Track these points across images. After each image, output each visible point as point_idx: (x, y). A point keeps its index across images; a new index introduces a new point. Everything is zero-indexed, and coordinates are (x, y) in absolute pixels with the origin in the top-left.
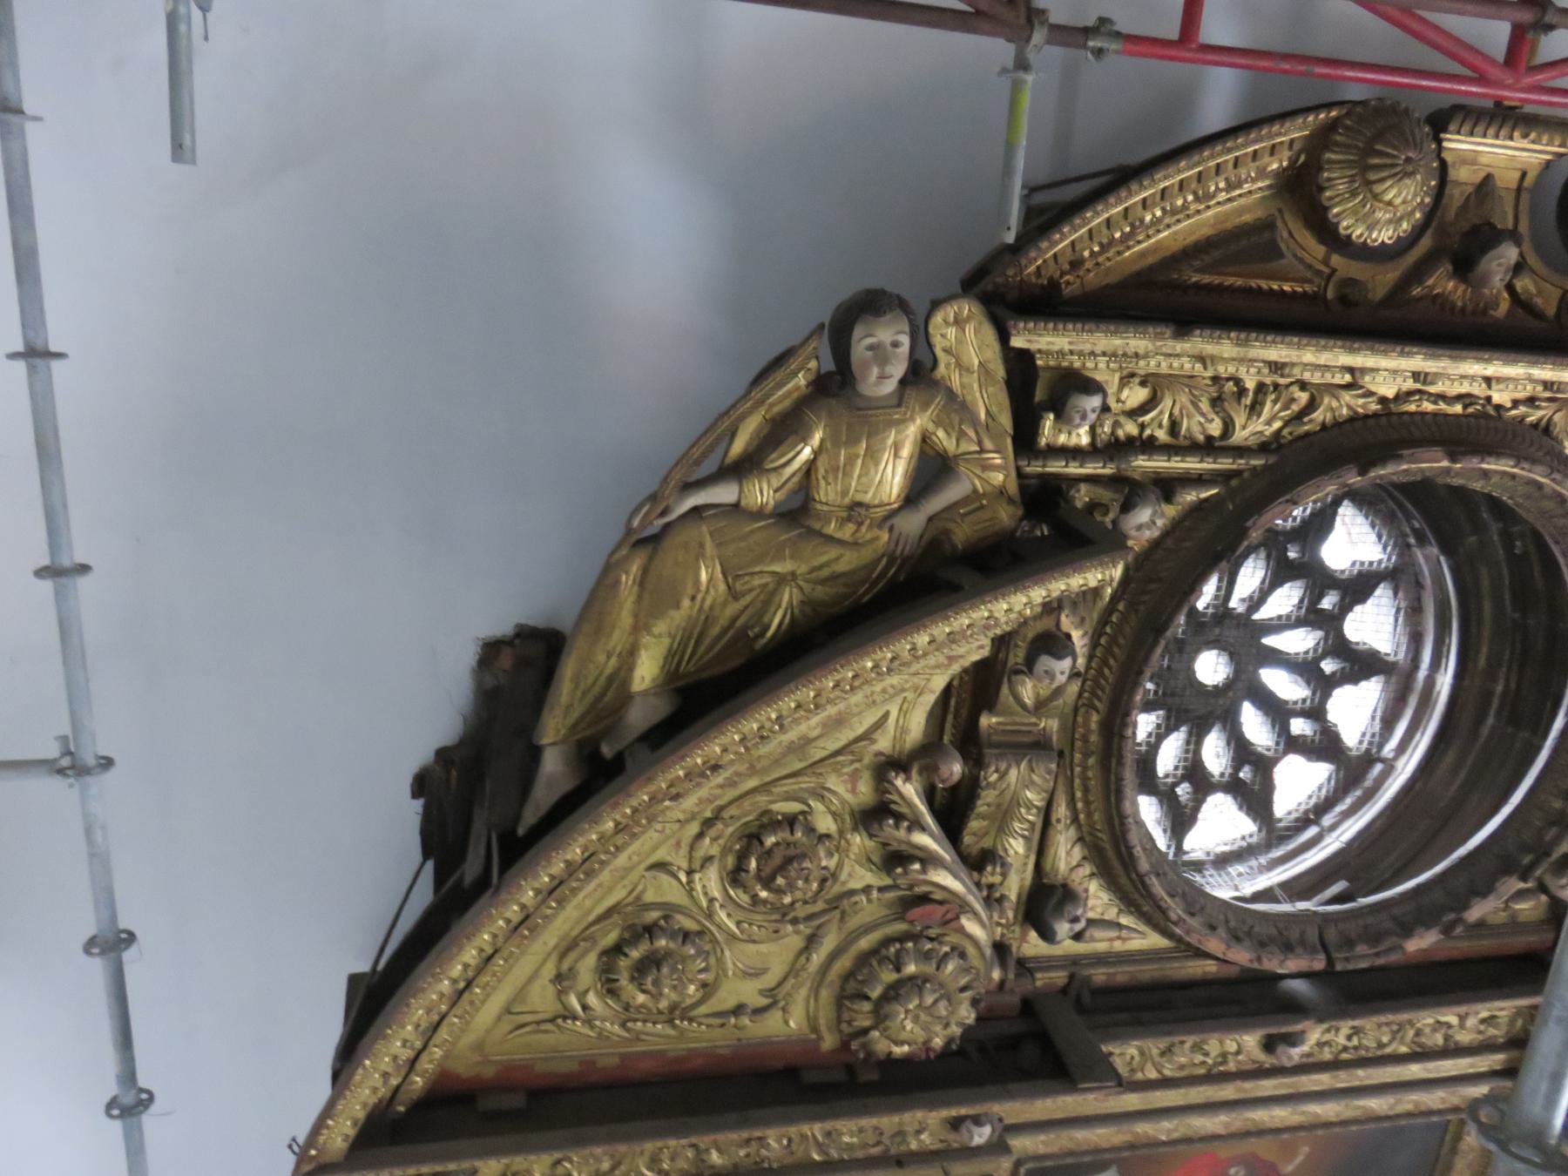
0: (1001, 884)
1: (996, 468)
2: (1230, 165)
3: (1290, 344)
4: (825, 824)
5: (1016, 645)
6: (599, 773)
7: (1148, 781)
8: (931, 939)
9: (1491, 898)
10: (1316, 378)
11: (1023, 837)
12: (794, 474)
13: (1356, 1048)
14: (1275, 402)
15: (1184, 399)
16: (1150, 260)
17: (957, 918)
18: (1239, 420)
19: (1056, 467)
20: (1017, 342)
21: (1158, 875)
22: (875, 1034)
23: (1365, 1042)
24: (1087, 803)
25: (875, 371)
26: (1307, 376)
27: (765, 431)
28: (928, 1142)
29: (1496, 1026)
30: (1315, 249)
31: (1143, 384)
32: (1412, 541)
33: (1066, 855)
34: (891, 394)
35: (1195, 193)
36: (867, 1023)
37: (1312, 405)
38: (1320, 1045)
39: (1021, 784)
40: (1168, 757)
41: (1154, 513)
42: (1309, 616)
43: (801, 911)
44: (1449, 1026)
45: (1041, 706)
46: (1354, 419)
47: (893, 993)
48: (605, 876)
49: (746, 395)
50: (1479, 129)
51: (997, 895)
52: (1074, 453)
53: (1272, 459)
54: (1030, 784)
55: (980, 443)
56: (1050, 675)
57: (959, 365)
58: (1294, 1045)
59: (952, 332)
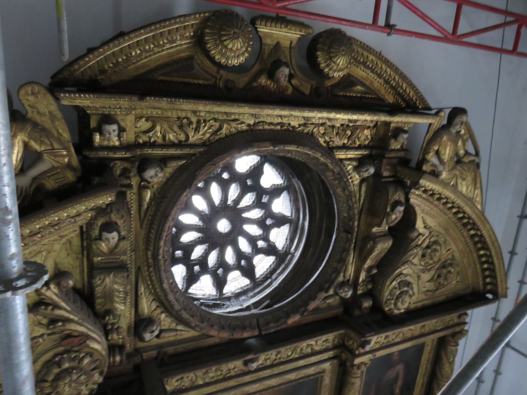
0: (118, 322)
1: (64, 156)
2: (167, 33)
3: (190, 103)
5: (94, 229)
9: (316, 300)
10: (220, 117)
11: (122, 303)
13: (280, 358)
14: (204, 127)
15: (166, 126)
16: (141, 71)
17: (85, 342)
18: (191, 134)
19: (104, 154)
20: (65, 102)
21: (185, 310)
23: (282, 356)
24: (153, 286)
26: (216, 116)
29: (329, 342)
32: (291, 176)
35: (153, 44)
37: (220, 128)
38: (266, 360)
44: (312, 345)
47: (58, 378)
50: (273, 25)
51: (116, 327)
52: (114, 149)
53: (206, 149)
54: (116, 283)
55: (52, 145)
57: (39, 113)
58: (253, 362)
59: (31, 98)
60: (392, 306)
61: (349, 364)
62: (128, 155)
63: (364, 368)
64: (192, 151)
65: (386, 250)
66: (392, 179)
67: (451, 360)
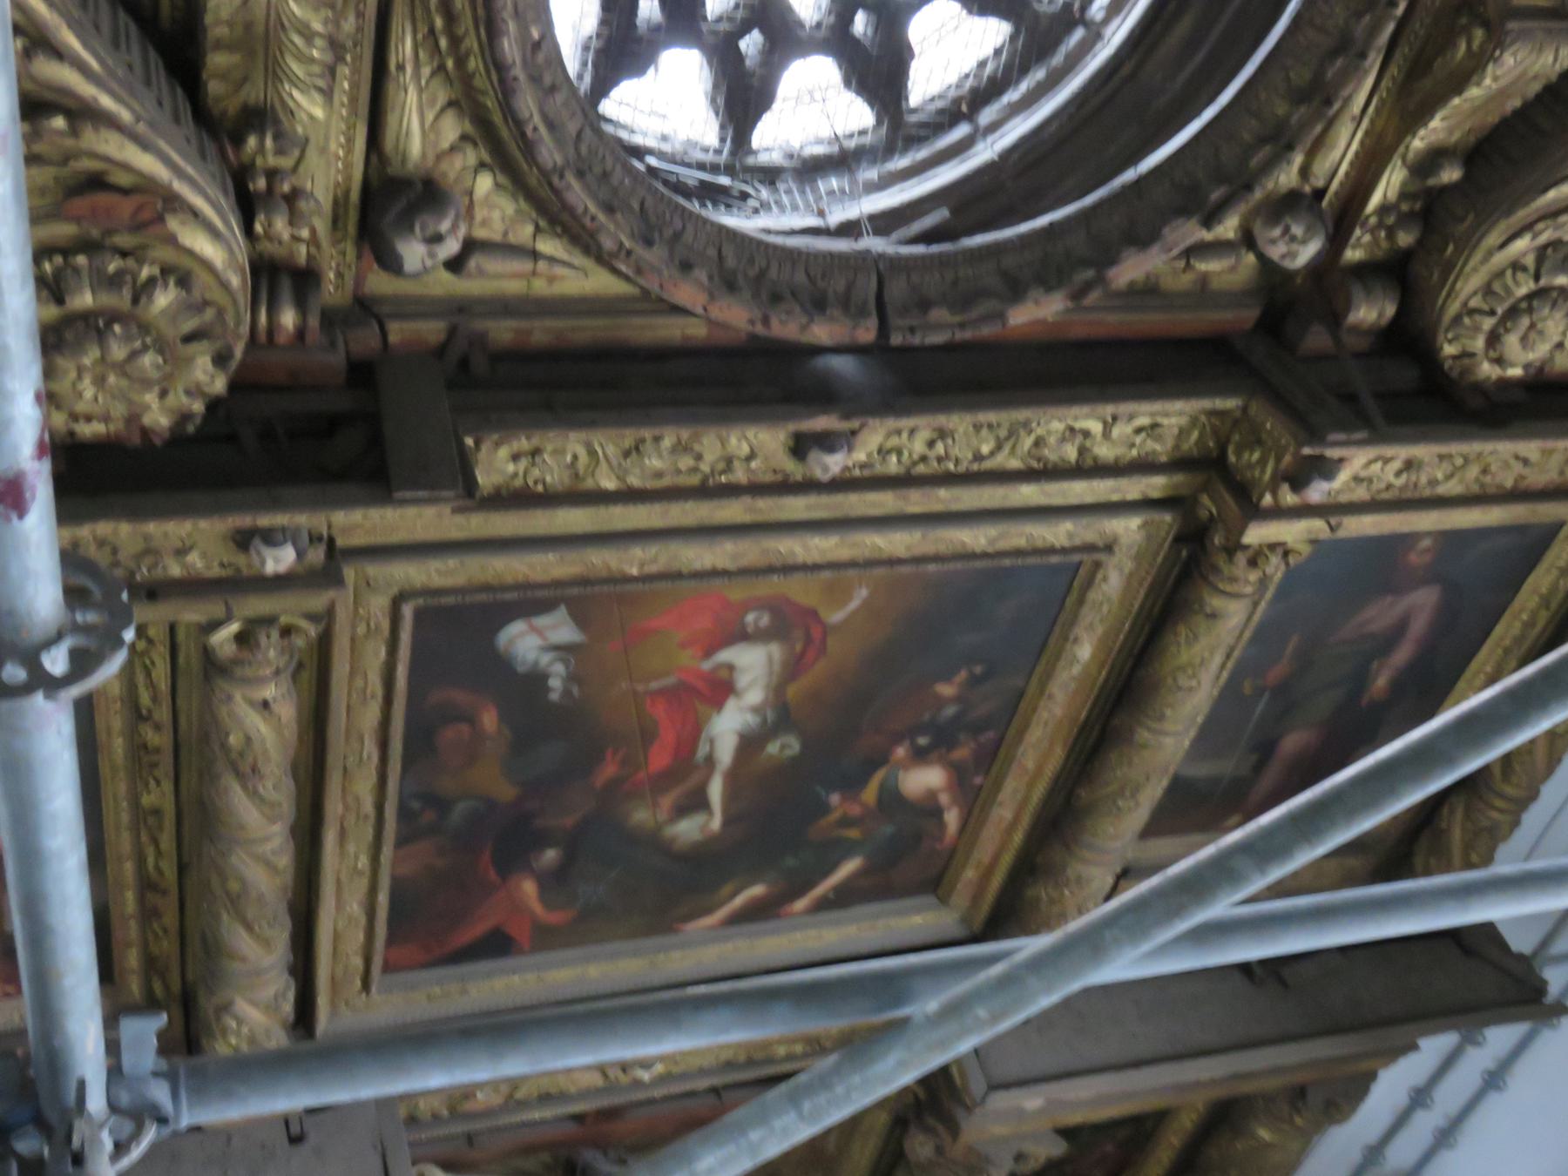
0: (295, 169)
8: (124, 254)
9: (1155, 249)
11: (320, 90)
13: (940, 459)
17: (160, 219)
21: (580, 174)
23: (956, 451)
24: (455, 41)
28: (199, 564)
29: (1159, 439)
38: (883, 452)
44: (1086, 434)
51: (286, 188)
58: (831, 449)
60: (1479, 343)
63: (1275, 567)
65: (1536, 87)
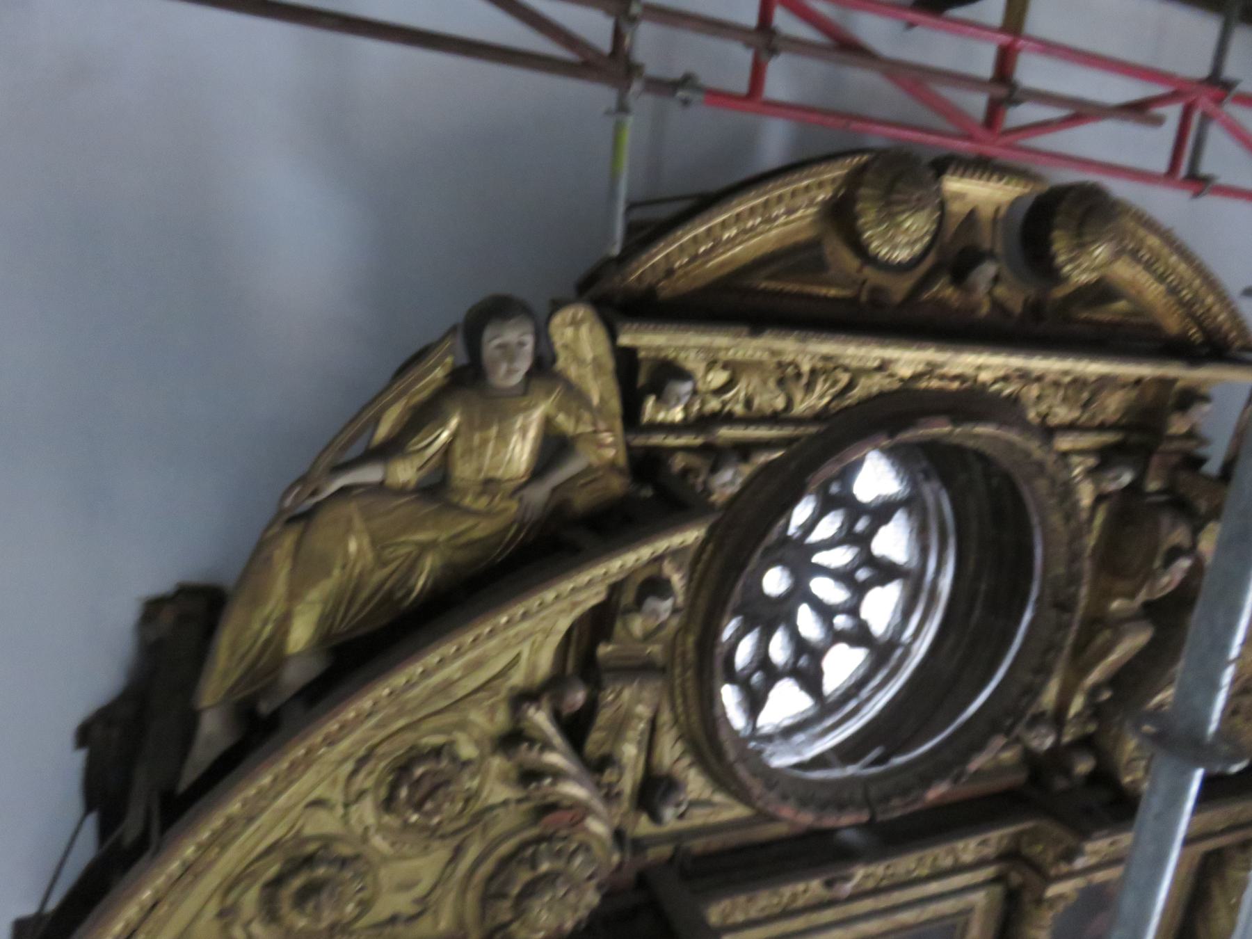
0: (618, 781)
4: (467, 750)
6: (261, 728)
7: (731, 676)
10: (855, 364)
12: (434, 455)
14: (825, 381)
15: (755, 381)
16: (727, 270)
17: (583, 819)
18: (798, 396)
19: (657, 440)
20: (625, 340)
22: (515, 926)
25: (503, 368)
27: (406, 419)
30: (848, 261)
31: (725, 366)
33: (670, 751)
34: (516, 387)
36: (506, 917)
37: (850, 386)
38: (866, 877)
39: (634, 702)
40: (744, 654)
41: (735, 474)
42: (846, 537)
43: (450, 828)
45: (649, 637)
46: (882, 395)
47: (530, 890)
48: (265, 818)
49: (388, 388)
52: (670, 428)
54: (639, 701)
56: (655, 613)
59: (569, 332)
60: (1139, 774)
61: (1027, 897)
62: (699, 441)
64: (801, 431)
66: (1163, 498)
67: (1234, 901)
